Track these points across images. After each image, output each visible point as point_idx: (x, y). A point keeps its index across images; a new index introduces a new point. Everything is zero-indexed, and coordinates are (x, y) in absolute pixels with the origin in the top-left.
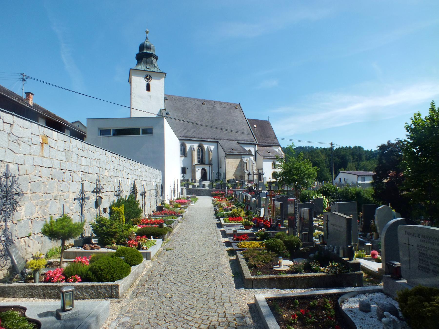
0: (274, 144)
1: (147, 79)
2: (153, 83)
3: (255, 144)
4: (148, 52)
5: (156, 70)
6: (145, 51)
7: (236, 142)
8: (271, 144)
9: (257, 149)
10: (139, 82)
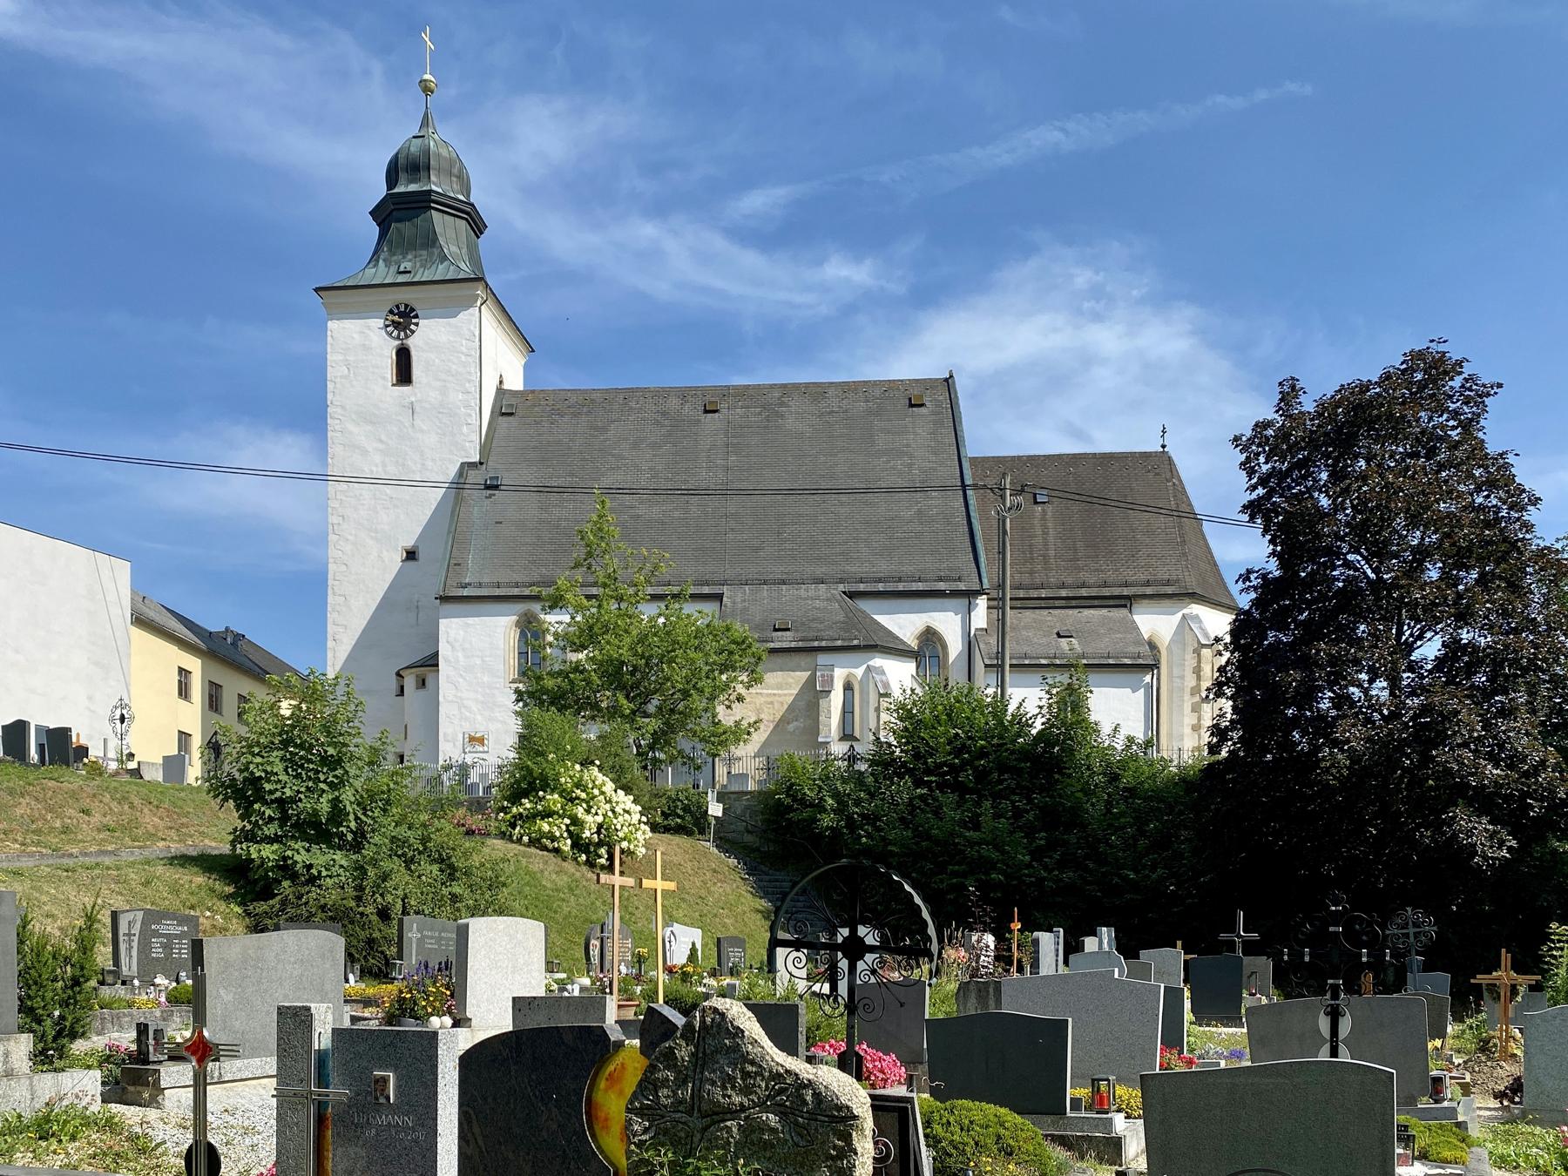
0: (1149, 591)
1: (396, 325)
2: (428, 336)
3: (971, 595)
4: (413, 187)
5: (440, 272)
7: (841, 587)
8: (1126, 592)
9: (981, 615)
10: (357, 343)
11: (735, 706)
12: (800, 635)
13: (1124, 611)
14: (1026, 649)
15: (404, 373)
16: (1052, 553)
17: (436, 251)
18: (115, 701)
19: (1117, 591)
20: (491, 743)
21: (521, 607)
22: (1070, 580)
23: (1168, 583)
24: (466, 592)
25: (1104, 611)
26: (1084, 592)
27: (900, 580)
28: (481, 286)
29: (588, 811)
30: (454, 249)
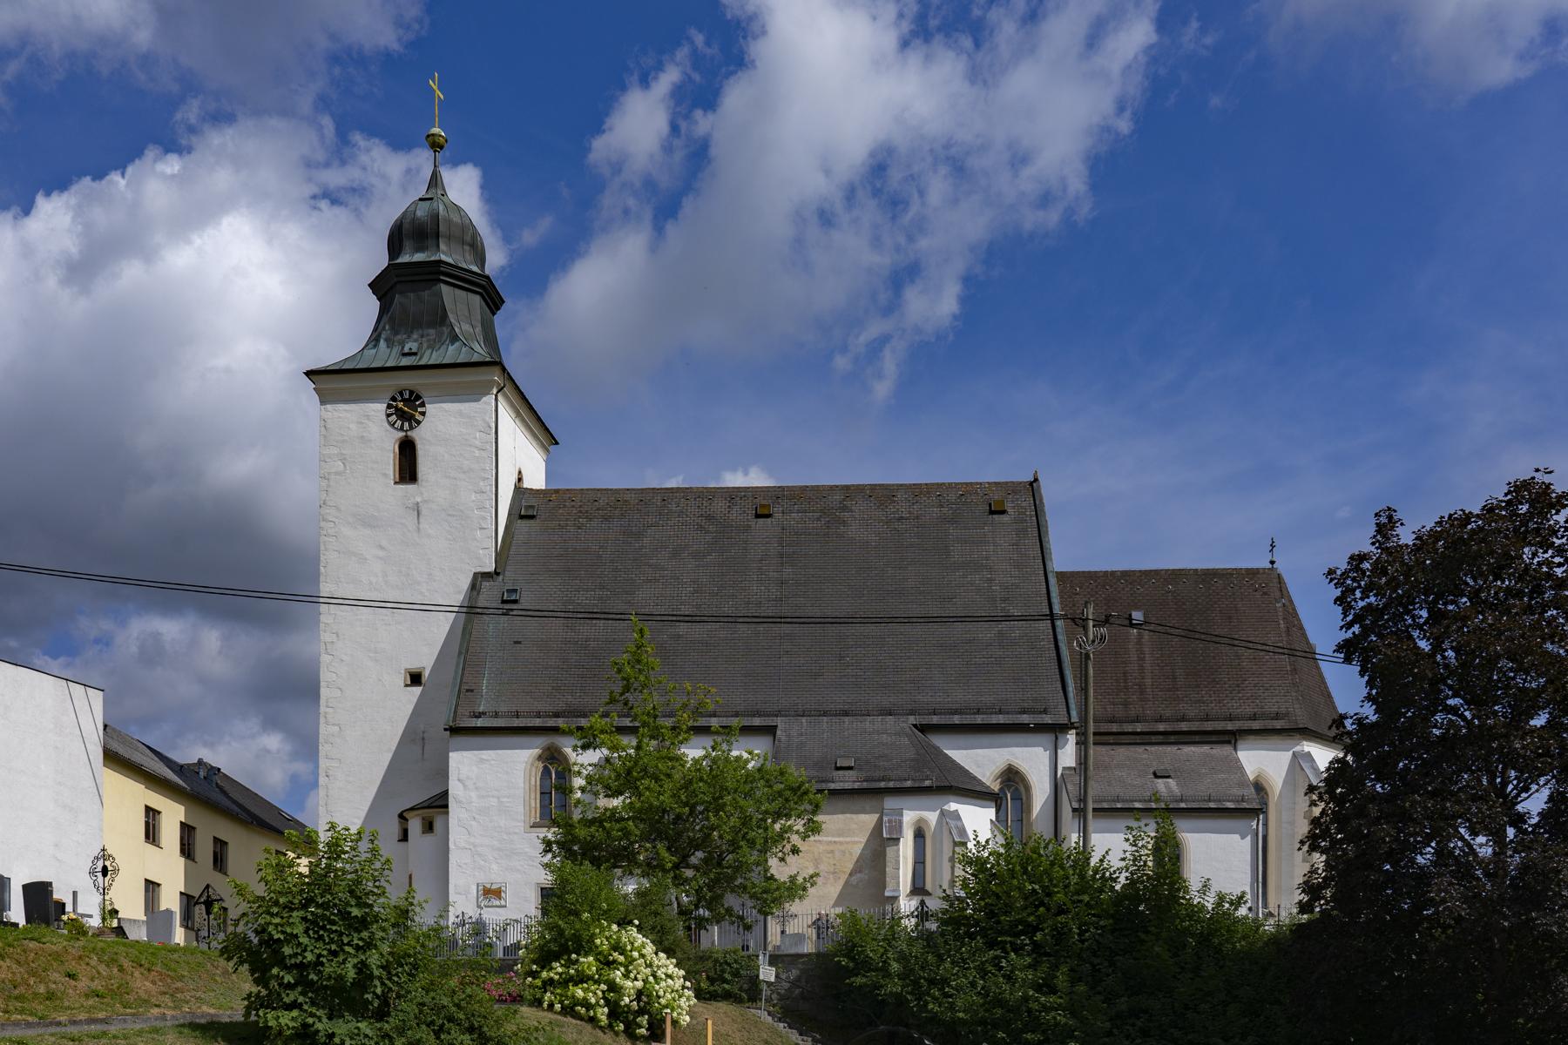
0: (1256, 725)
1: (402, 415)
4: (419, 257)
5: (450, 353)
6: (405, 258)
7: (912, 719)
8: (1230, 726)
9: (1068, 755)
11: (790, 859)
12: (863, 775)
13: (1227, 749)
14: (1117, 790)
15: (408, 469)
16: (1148, 681)
17: (446, 330)
18: (96, 851)
19: (1219, 726)
20: (509, 896)
21: (542, 741)
22: (1168, 713)
23: (1277, 717)
24: (480, 723)
25: (1206, 749)
26: (1184, 726)
27: (978, 712)
28: (497, 369)
29: (626, 976)
30: (466, 327)
